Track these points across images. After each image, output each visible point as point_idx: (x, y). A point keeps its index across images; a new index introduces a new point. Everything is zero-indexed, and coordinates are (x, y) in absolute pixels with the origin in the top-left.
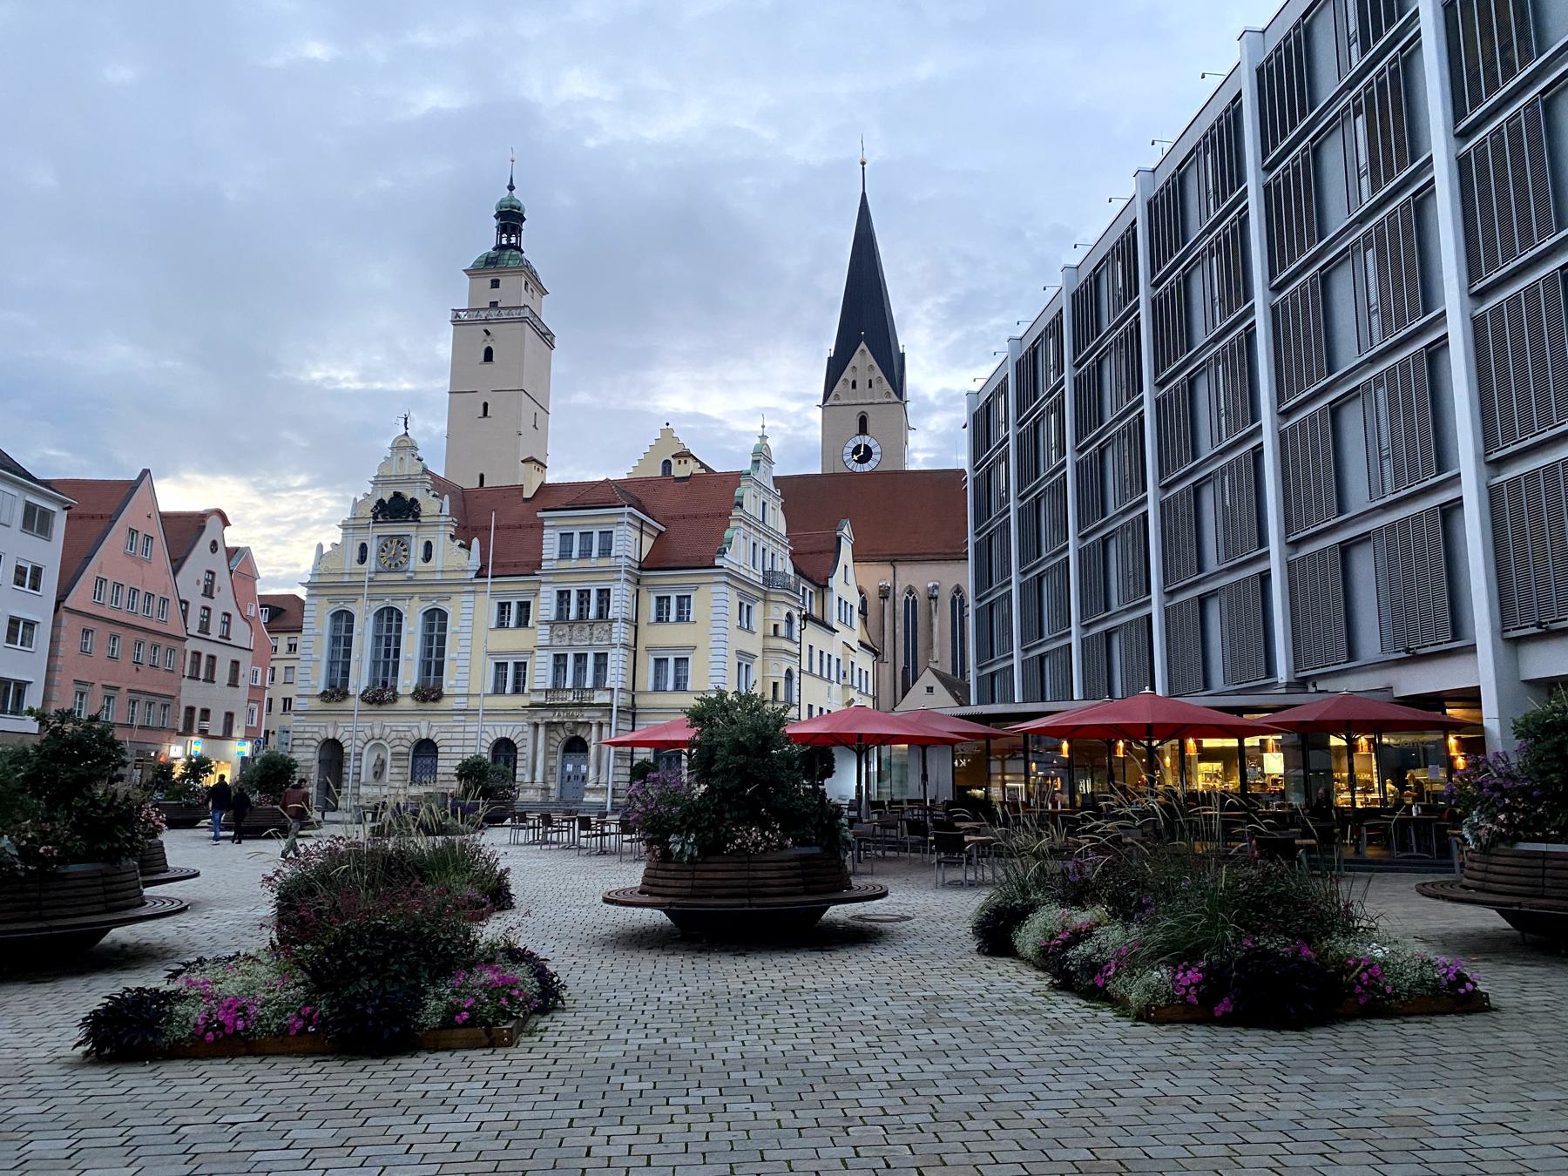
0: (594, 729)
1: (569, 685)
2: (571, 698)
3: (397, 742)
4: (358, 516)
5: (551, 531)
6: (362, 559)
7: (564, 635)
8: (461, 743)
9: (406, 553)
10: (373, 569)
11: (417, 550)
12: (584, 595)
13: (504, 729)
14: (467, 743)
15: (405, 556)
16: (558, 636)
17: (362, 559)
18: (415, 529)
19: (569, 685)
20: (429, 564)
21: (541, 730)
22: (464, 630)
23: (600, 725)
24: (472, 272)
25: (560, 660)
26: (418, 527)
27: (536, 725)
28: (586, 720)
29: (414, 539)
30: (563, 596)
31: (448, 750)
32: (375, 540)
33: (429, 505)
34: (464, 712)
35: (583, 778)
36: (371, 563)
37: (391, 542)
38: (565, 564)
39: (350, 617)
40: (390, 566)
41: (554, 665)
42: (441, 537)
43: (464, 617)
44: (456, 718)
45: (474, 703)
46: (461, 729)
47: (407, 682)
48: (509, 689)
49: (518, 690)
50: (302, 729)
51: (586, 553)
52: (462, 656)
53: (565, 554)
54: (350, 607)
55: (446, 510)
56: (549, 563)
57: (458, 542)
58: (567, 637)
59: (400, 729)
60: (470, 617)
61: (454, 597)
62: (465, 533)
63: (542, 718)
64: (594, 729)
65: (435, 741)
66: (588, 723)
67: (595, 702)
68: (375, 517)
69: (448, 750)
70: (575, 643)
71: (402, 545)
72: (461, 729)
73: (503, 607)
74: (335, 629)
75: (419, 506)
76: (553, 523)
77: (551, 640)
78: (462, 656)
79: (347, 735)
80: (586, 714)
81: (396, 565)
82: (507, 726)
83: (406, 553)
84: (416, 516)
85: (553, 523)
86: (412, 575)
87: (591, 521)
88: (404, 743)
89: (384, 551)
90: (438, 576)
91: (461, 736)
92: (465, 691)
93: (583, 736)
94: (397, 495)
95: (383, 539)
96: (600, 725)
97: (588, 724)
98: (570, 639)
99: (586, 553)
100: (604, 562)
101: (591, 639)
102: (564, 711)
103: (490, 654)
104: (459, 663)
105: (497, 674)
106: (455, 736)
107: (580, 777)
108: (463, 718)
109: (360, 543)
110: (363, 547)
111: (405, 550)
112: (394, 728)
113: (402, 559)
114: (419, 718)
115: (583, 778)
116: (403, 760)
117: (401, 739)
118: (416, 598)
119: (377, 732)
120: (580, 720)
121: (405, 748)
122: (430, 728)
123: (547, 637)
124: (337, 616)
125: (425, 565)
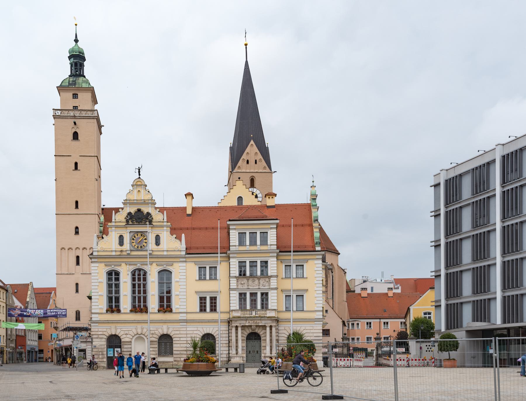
0: (268, 329)
1: (248, 307)
2: (255, 314)
4: (117, 221)
5: (234, 231)
6: (121, 243)
7: (244, 283)
8: (185, 336)
10: (128, 249)
11: (151, 239)
12: (253, 264)
13: (208, 329)
15: (146, 243)
16: (242, 284)
17: (121, 243)
19: (248, 307)
20: (159, 247)
21: (239, 329)
22: (181, 280)
23: (271, 327)
24: (61, 89)
25: (242, 296)
26: (152, 227)
27: (237, 327)
28: (263, 324)
29: (150, 234)
30: (242, 265)
31: (178, 339)
32: (128, 234)
33: (157, 217)
34: (186, 321)
35: (257, 352)
36: (127, 246)
37: (137, 235)
38: (242, 248)
39: (117, 274)
40: (138, 247)
41: (239, 298)
42: (165, 233)
43: (181, 274)
44: (181, 324)
45: (190, 317)
46: (185, 329)
47: (153, 306)
48: (208, 309)
49: (213, 309)
51: (253, 242)
52: (181, 294)
53: (241, 243)
54: (117, 268)
55: (165, 220)
56: (234, 248)
57: (175, 236)
58: (246, 285)
61: (175, 264)
62: (175, 231)
63: (240, 324)
64: (268, 329)
65: (171, 335)
66: (265, 326)
67: (268, 316)
68: (127, 221)
69: (178, 339)
70: (250, 287)
72: (185, 329)
73: (202, 269)
74: (110, 279)
75: (151, 216)
76: (234, 227)
77: (237, 286)
78: (181, 294)
79: (122, 333)
80: (263, 322)
81: (141, 247)
82: (210, 327)
84: (151, 222)
85: (234, 227)
86: (151, 252)
87: (258, 227)
88: (155, 336)
90: (165, 253)
91: (185, 332)
92: (185, 311)
93: (258, 332)
94: (139, 210)
95: (132, 234)
96: (271, 327)
97: (264, 327)
98: (248, 286)
99: (253, 242)
100: (264, 248)
101: (259, 285)
102: (251, 320)
103: (196, 292)
104: (180, 297)
105: (201, 303)
106: (182, 332)
107: (256, 351)
108: (185, 324)
109: (119, 235)
110: (121, 238)
111: (145, 239)
113: (145, 245)
115: (257, 352)
116: (155, 344)
117: (153, 334)
118: (154, 264)
119: (139, 331)
120: (260, 324)
121: (155, 339)
122: (168, 328)
123: (235, 284)
124: (110, 273)
125: (157, 247)
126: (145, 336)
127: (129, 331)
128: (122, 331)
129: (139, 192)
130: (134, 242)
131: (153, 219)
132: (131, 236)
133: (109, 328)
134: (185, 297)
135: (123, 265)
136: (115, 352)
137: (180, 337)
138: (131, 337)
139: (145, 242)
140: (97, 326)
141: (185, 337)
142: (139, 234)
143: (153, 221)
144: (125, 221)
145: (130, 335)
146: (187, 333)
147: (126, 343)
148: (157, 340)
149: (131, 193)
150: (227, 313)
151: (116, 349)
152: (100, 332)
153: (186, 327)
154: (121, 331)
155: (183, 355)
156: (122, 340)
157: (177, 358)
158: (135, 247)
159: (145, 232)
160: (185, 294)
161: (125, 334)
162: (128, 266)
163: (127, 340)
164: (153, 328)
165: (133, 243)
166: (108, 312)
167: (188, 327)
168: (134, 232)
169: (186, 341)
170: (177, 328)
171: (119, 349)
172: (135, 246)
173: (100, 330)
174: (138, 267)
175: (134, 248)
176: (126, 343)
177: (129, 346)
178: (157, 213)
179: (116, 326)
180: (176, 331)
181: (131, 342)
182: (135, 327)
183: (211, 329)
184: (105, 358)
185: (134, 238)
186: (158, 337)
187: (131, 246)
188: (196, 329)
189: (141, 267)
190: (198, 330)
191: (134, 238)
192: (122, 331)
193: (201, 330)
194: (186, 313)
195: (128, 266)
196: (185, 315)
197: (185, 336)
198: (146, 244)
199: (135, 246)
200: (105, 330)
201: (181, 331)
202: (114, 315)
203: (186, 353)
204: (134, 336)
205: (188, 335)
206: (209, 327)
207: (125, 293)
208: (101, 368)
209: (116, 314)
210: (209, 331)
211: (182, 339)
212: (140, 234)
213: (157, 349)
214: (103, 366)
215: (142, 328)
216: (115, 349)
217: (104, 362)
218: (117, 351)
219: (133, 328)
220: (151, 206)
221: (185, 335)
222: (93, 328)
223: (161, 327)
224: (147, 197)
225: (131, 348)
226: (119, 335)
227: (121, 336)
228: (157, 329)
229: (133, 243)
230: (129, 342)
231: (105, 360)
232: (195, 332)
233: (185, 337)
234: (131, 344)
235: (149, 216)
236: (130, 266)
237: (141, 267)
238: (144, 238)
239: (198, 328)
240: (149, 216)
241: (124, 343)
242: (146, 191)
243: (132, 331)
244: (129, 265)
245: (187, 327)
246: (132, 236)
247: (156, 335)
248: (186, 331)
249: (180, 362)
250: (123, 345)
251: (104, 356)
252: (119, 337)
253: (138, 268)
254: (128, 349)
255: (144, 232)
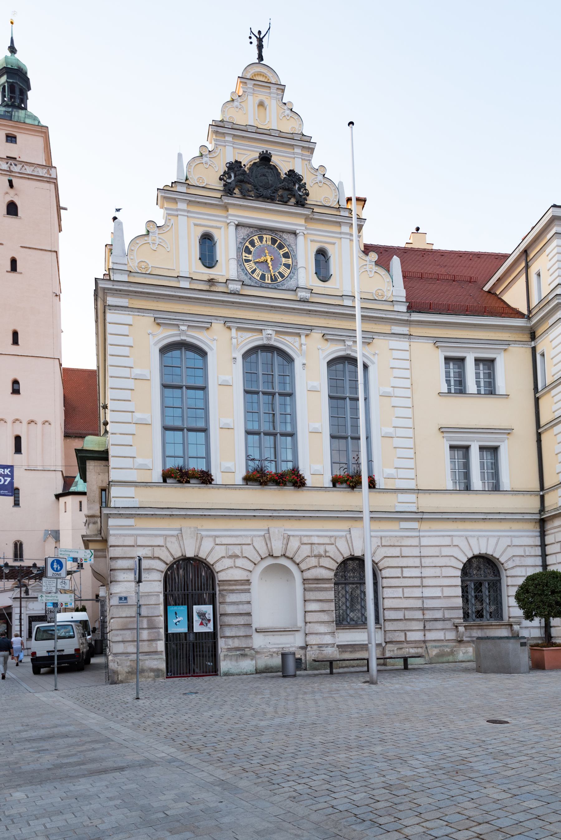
3: (313, 561)
8: (417, 562)
9: (290, 261)
14: (426, 562)
15: (287, 266)
18: (302, 221)
26: (308, 219)
29: (300, 239)
31: (397, 572)
37: (261, 239)
40: (263, 277)
44: (404, 525)
46: (415, 542)
50: (129, 541)
59: (316, 540)
60: (407, 374)
69: (397, 572)
71: (281, 247)
72: (415, 542)
79: (220, 551)
81: (274, 279)
83: (290, 261)
84: (301, 203)
89: (250, 252)
91: (415, 551)
95: (244, 232)
103: (442, 430)
106: (406, 551)
108: (415, 525)
109: (200, 231)
111: (286, 256)
112: (305, 540)
113: (286, 272)
114: (345, 525)
116: (325, 589)
117: (319, 556)
119: (277, 548)
126: (294, 562)
127: (244, 547)
128: (217, 544)
129: (261, 108)
130: (251, 260)
131: (308, 195)
132: (239, 240)
133: (172, 536)
134: (409, 443)
135: (218, 326)
136: (196, 617)
137: (401, 567)
138: (250, 566)
139: (285, 265)
140: (130, 527)
141: (416, 567)
142: (267, 237)
143: (308, 202)
144: (222, 189)
145: (246, 559)
146: (422, 555)
147: (234, 587)
148: (331, 575)
149: (236, 103)
150: (531, 495)
151: (196, 608)
152: (141, 549)
153: (417, 534)
154: (217, 547)
155: (414, 623)
156: (221, 577)
157: (397, 634)
158: (254, 275)
159: (283, 231)
160: (410, 433)
161: (230, 557)
162: (234, 331)
163: (238, 575)
164: (318, 536)
165: (248, 261)
166: (168, 481)
167: (424, 536)
168: (251, 230)
169: (419, 580)
170: (391, 536)
171: (208, 609)
172: (253, 272)
173: (140, 541)
174: (269, 339)
175: (250, 279)
176: (234, 587)
177: (243, 597)
178: (321, 182)
179: (199, 528)
180: (390, 546)
181: (248, 582)
182: (262, 533)
183: (493, 541)
184: (160, 640)
185: (250, 246)
186: (334, 566)
187: (240, 270)
188: (447, 541)
189: (276, 340)
190: (454, 544)
191: (250, 246)
192: (217, 544)
193: (463, 543)
194: (418, 491)
195: (234, 331)
196: (412, 497)
197: (417, 562)
198: (289, 271)
199: (253, 272)
200: (160, 541)
201: (403, 548)
202: (191, 489)
203: (421, 617)
204: (259, 562)
205: (423, 560)
206: (484, 536)
207: (226, 421)
208: (146, 674)
209: (196, 490)
210: (487, 549)
211: (407, 572)
212: (268, 236)
213: (332, 606)
214: (155, 667)
215: (286, 536)
216: (195, 607)
217: (156, 652)
218: (202, 615)
219: (255, 536)
220: (302, 155)
221: (418, 560)
222: (114, 535)
223: (344, 534)
224: (287, 127)
225: (249, 603)
226: (211, 560)
227: (217, 564)
228: (333, 540)
229: (248, 261)
230: (242, 585)
231: (161, 646)
232: (446, 551)
233: (416, 567)
234: (248, 591)
235: (297, 186)
236: (240, 333)
237: (276, 340)
238: (281, 252)
239: (454, 538)
240: (297, 186)
241: (226, 588)
242: (285, 107)
243: (251, 546)
244: (238, 329)
245: (421, 534)
246: (244, 239)
247: (329, 559)
248: (418, 549)
249: (405, 645)
250: (224, 593)
251: (159, 633)
252: (208, 568)
253: (265, 342)
254: (241, 607)
255: (281, 234)
